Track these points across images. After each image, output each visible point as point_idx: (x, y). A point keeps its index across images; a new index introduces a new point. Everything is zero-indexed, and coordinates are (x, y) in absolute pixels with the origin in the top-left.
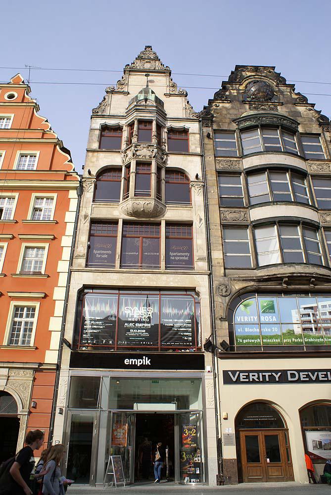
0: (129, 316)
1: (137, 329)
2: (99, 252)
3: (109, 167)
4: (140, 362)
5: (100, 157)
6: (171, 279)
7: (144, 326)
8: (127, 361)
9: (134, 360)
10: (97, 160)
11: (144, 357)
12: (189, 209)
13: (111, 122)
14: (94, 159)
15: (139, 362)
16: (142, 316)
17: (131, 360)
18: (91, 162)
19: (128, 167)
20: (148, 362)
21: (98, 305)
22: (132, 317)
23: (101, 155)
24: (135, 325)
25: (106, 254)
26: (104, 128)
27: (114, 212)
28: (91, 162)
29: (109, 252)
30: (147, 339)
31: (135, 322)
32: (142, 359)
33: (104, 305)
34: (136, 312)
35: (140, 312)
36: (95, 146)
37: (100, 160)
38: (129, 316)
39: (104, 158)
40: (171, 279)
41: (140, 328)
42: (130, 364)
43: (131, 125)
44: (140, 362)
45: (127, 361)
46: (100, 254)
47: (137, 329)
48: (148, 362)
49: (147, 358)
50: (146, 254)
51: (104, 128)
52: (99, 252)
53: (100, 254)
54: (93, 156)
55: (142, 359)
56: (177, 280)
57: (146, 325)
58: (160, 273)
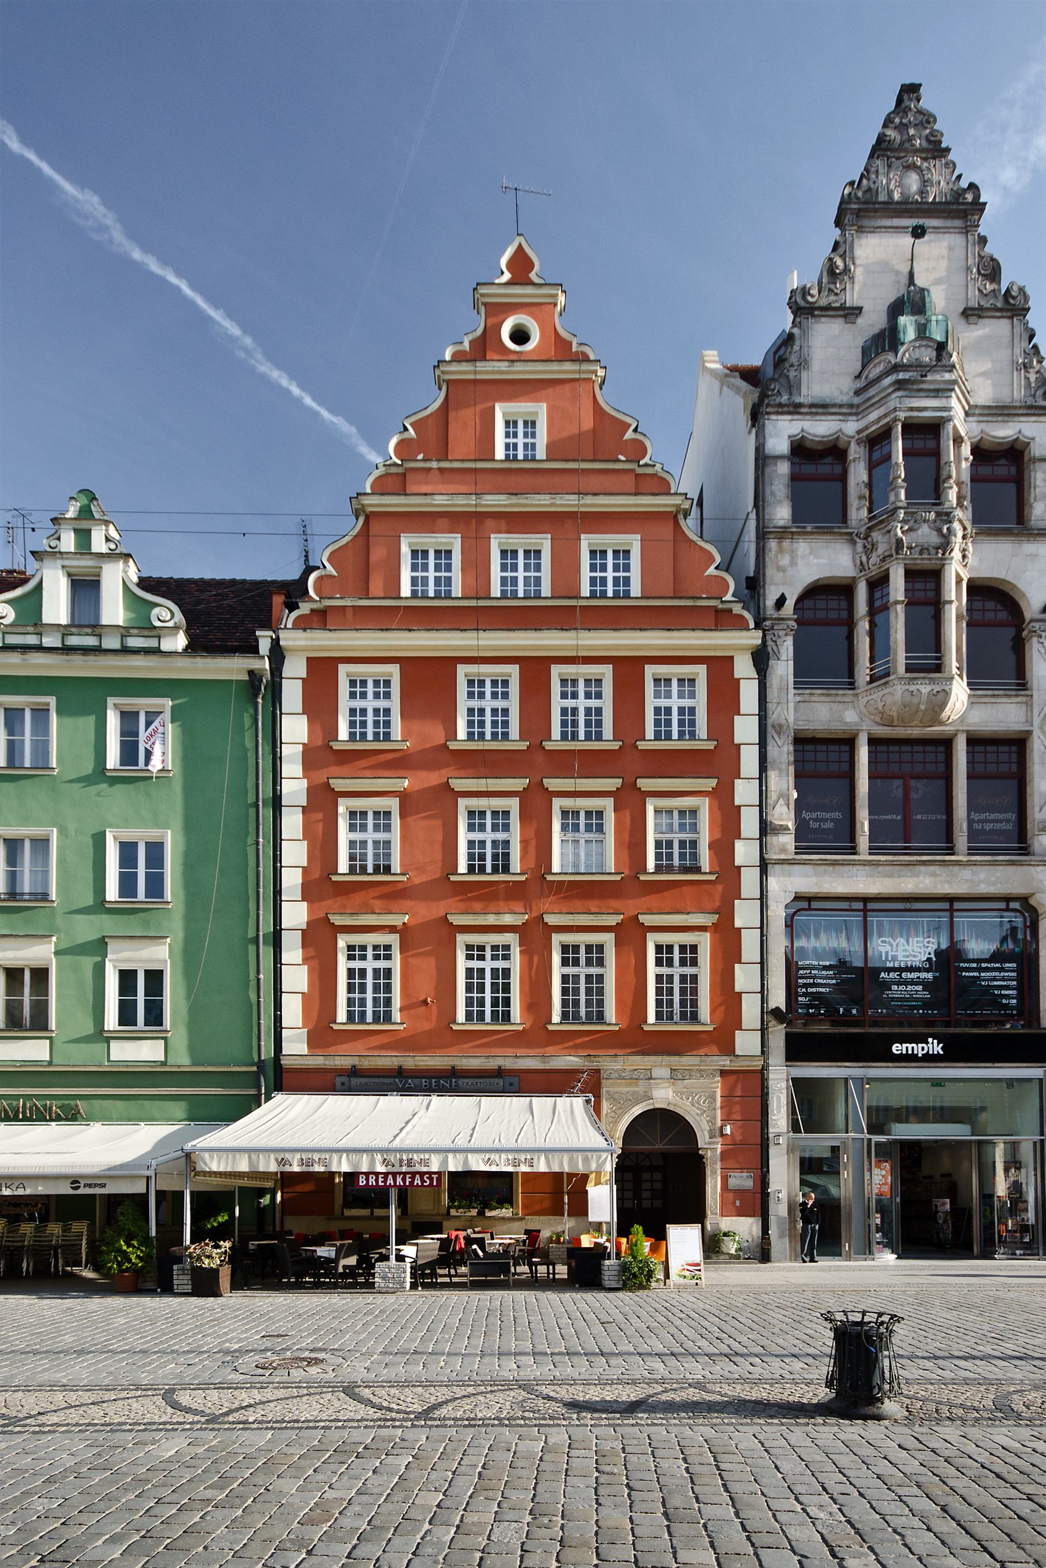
0: (887, 957)
1: (906, 983)
2: (814, 815)
3: (819, 583)
4: (923, 1049)
5: (799, 553)
6: (982, 876)
7: (918, 978)
8: (896, 1048)
9: (910, 1046)
10: (793, 563)
11: (930, 1040)
12: (1024, 699)
13: (820, 428)
14: (785, 561)
15: (919, 1049)
16: (915, 956)
17: (904, 1045)
18: (780, 569)
19: (879, 583)
20: (935, 1047)
21: (823, 935)
22: (894, 959)
23: (802, 546)
24: (900, 975)
25: (832, 820)
26: (800, 449)
27: (847, 713)
28: (780, 569)
29: (837, 815)
30: (926, 1004)
31: (901, 970)
32: (927, 1043)
33: (834, 934)
34: (901, 948)
35: (910, 948)
36: (782, 513)
37: (800, 561)
38: (887, 957)
39: (810, 554)
40: (982, 876)
41: (912, 982)
42: (904, 1052)
43: (877, 441)
44: (923, 1049)
45: (896, 1048)
46: (816, 820)
47: (906, 983)
48: (935, 1047)
49: (935, 1041)
50: (919, 817)
51: (800, 449)
52: (814, 815)
53: (816, 820)
54: (781, 551)
55: (927, 1043)
56: (993, 879)
57: (923, 975)
58: (958, 863)
